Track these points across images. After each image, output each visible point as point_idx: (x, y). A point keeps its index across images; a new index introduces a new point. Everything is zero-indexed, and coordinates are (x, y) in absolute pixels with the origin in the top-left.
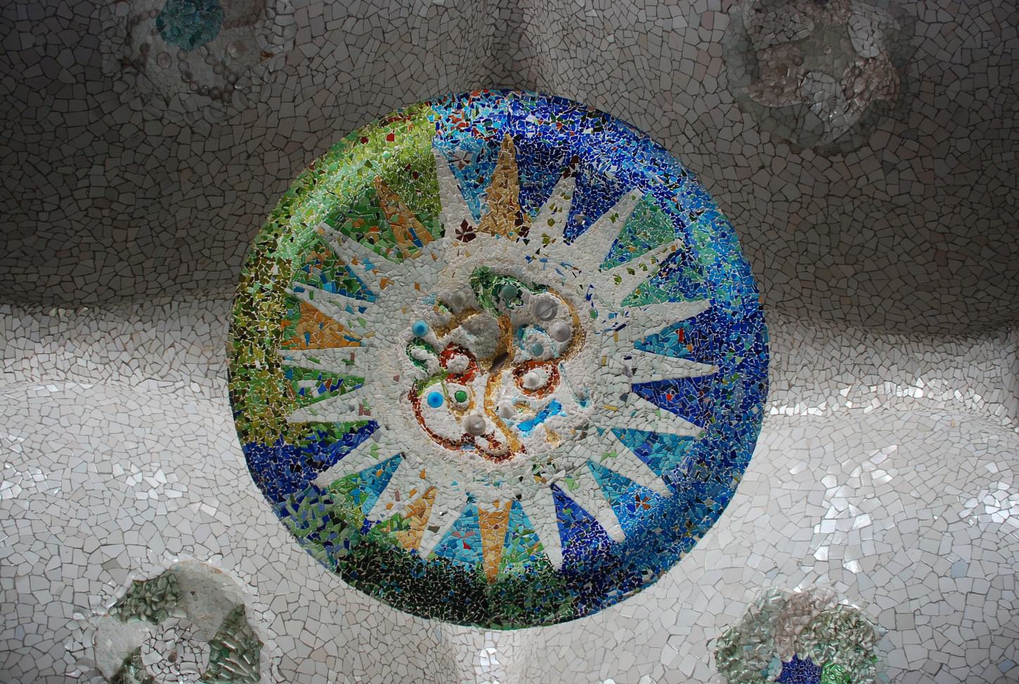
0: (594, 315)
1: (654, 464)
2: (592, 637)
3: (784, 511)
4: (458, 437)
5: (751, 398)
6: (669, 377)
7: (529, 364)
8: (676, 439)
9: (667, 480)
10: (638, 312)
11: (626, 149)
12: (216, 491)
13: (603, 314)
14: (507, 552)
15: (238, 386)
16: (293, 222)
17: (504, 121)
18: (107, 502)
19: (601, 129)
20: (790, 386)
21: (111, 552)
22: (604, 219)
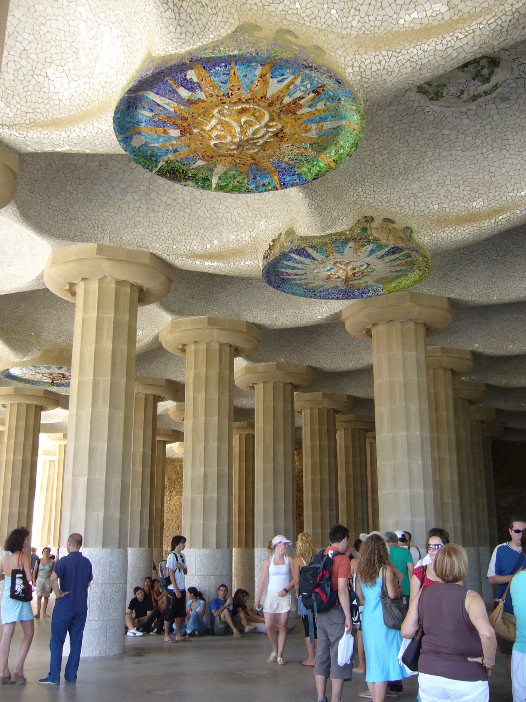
8: (285, 268)
12: (450, 143)
18: (506, 126)
21: (504, 105)
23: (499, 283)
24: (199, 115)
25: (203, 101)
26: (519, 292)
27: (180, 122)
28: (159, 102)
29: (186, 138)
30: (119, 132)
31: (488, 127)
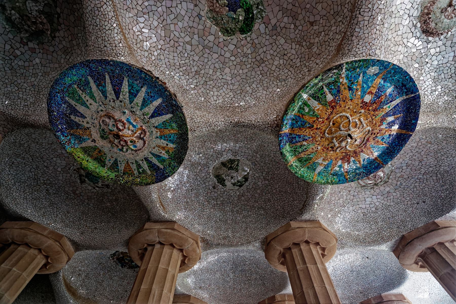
0: (102, 111)
1: (138, 91)
2: (217, 84)
3: (176, 16)
4: (142, 141)
5: (109, 64)
6: (112, 89)
7: (117, 128)
8: (129, 85)
9: (142, 87)
10: (97, 99)
11: (55, 104)
13: (100, 108)
14: (170, 128)
15: (143, 184)
16: (105, 175)
17: (63, 133)
19: (53, 110)
20: (105, 46)
22: (77, 108)
23: (14, 187)
24: (372, 119)
25: (379, 126)
26: (13, 202)
27: (374, 107)
28: (393, 103)
29: (359, 103)
30: (396, 69)
31: (199, 183)
